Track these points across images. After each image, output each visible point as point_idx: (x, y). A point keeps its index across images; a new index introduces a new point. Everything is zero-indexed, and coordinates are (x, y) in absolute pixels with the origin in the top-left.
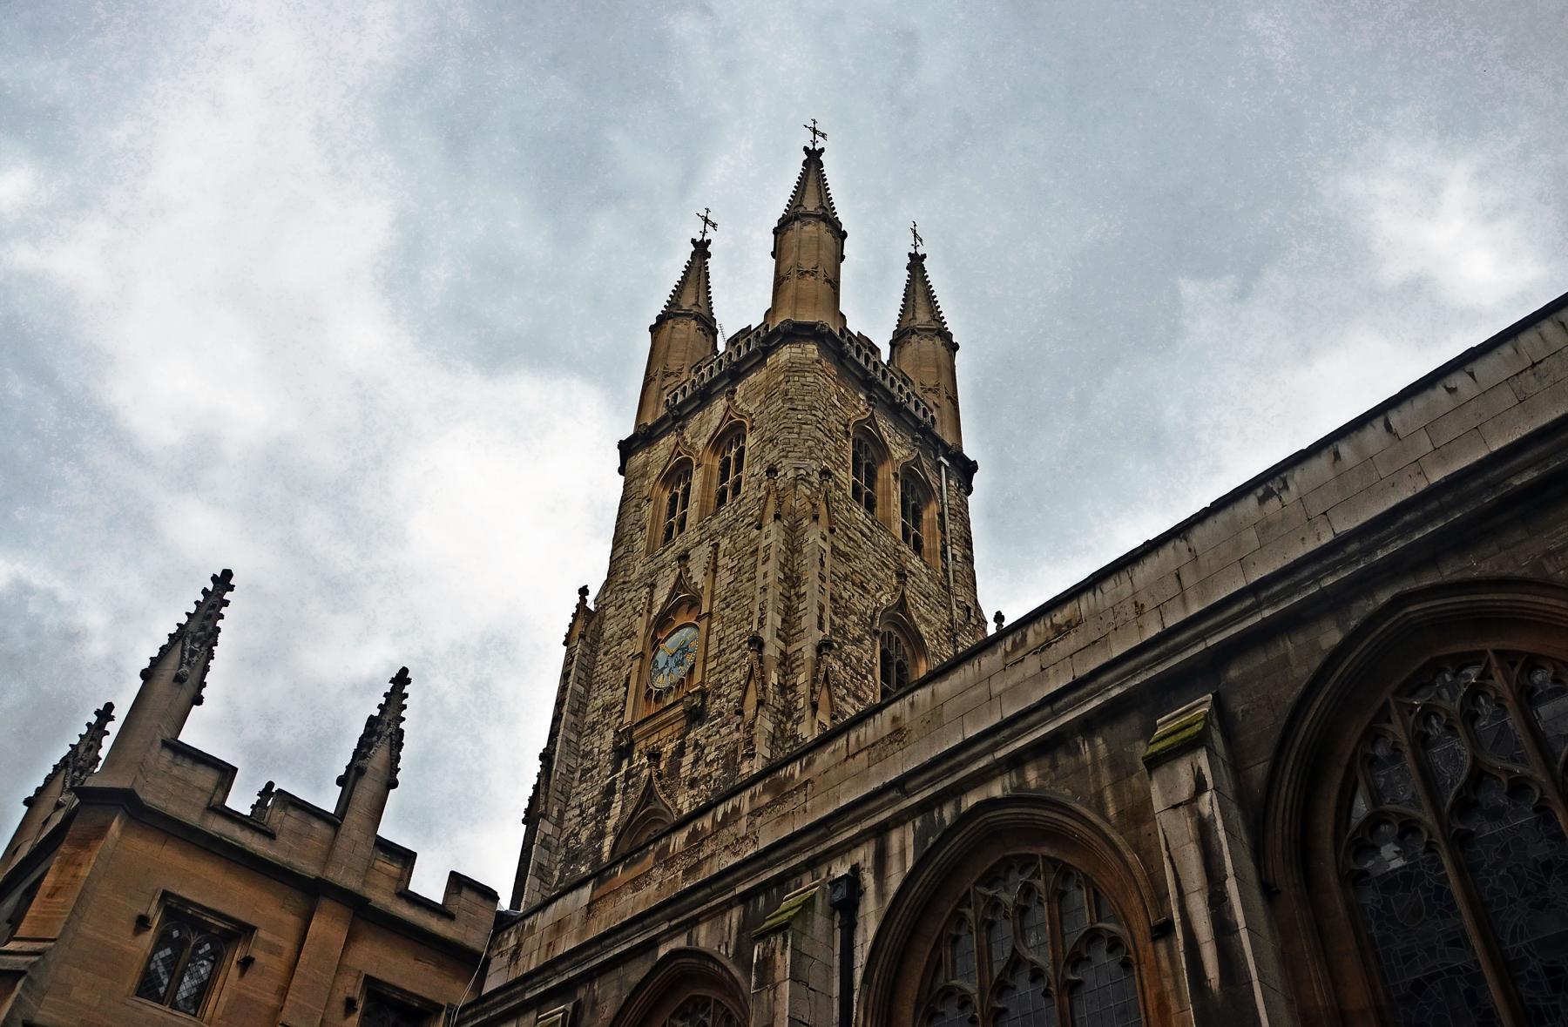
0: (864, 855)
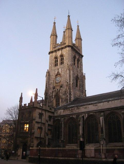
0: (84, 115)
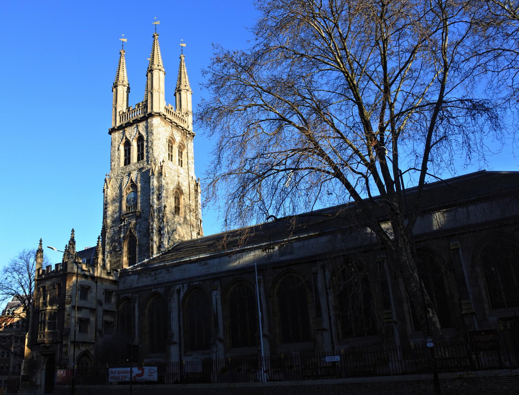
0: (181, 286)
